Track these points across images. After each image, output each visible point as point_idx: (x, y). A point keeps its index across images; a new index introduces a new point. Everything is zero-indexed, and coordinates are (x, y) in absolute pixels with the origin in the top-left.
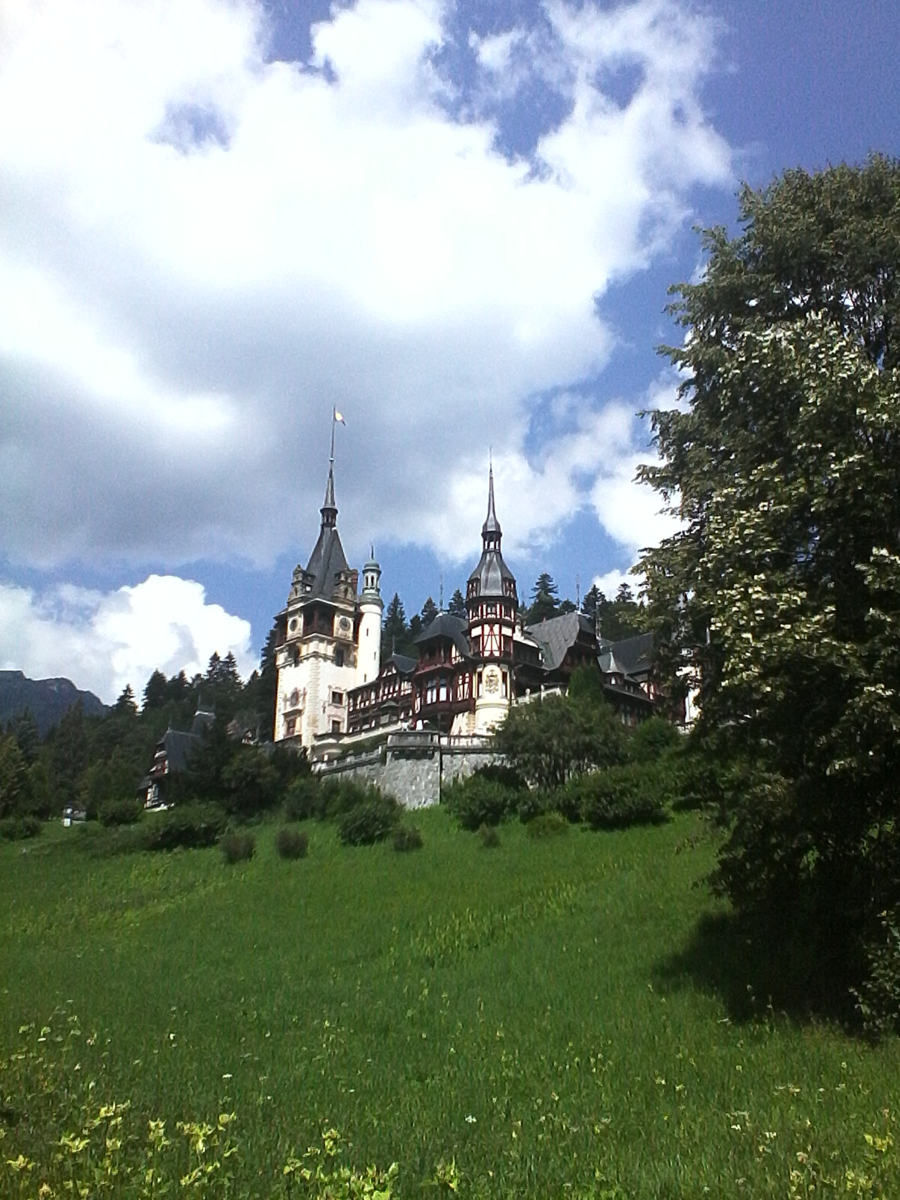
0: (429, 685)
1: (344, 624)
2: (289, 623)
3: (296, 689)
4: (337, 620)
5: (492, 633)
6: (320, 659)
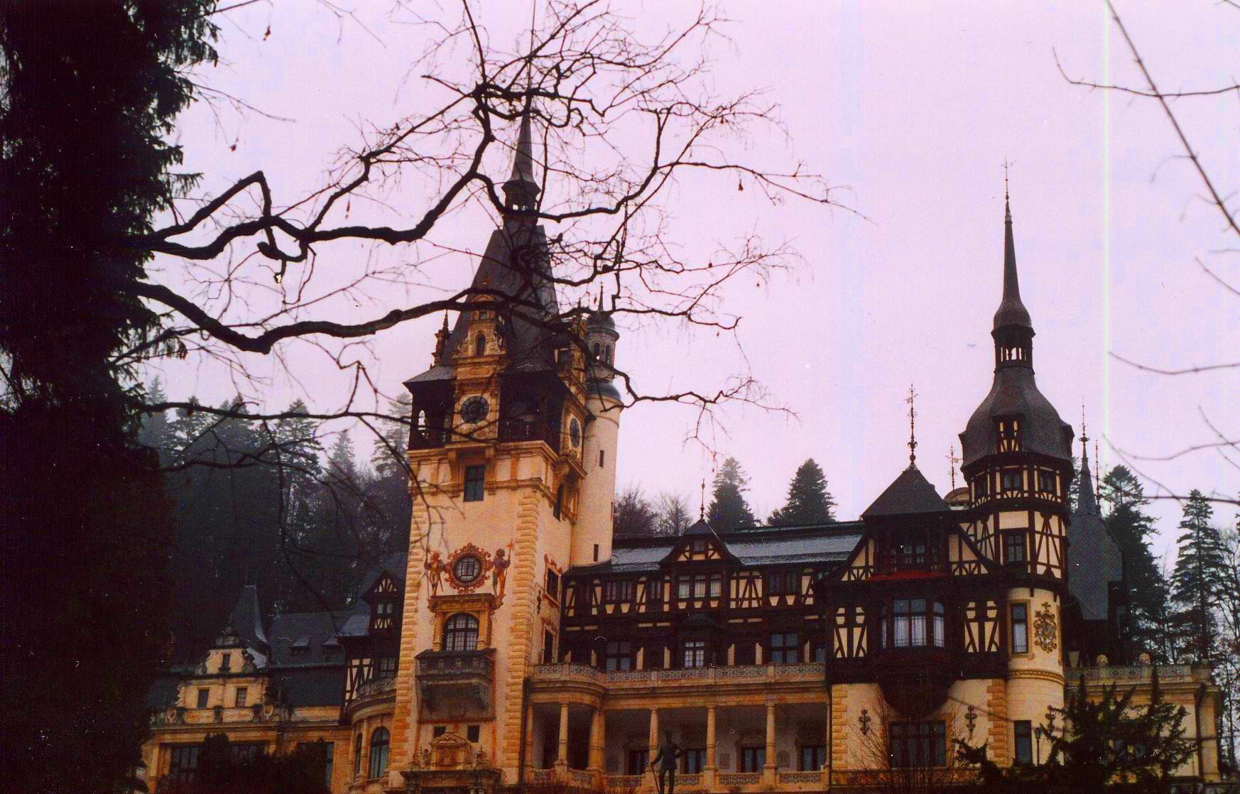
5: (1046, 530)
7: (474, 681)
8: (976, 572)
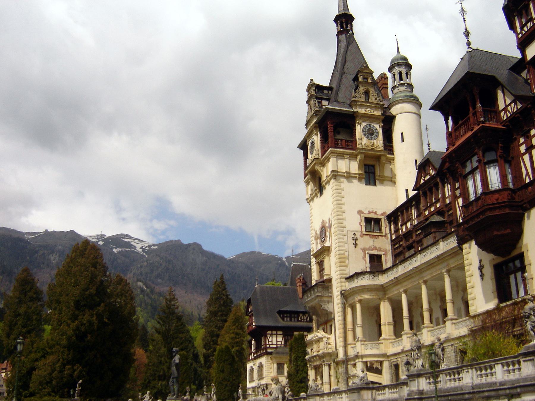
0: (468, 169)
1: (370, 133)
2: (309, 147)
3: (323, 222)
4: (359, 129)
6: (342, 179)
7: (317, 300)
8: (515, 110)
